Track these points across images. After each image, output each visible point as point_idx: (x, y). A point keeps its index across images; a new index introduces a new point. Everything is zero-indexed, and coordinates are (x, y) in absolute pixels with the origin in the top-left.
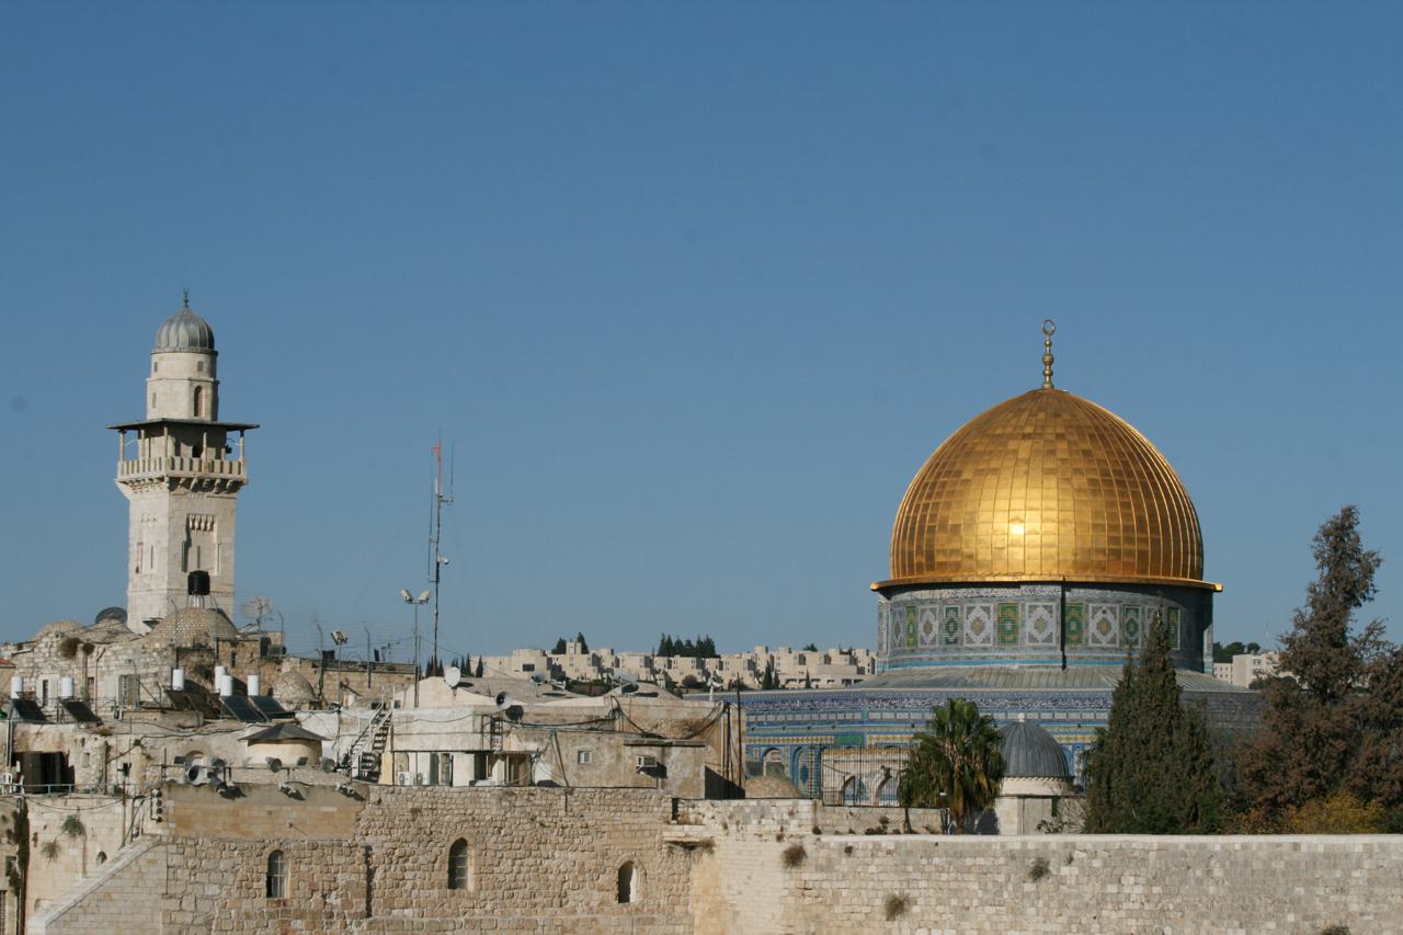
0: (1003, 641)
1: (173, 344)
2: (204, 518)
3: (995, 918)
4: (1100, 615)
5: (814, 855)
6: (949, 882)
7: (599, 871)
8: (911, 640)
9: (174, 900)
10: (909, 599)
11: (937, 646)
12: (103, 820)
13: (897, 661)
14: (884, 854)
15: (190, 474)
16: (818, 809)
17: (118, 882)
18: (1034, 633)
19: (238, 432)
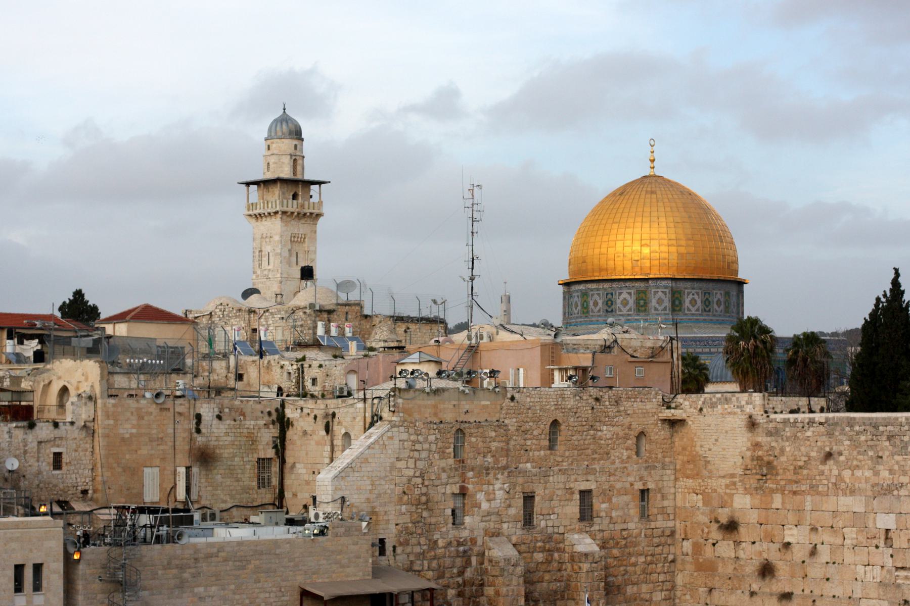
0: (639, 311)
1: (280, 134)
2: (300, 236)
3: (902, 463)
4: (691, 296)
5: (765, 426)
6: (867, 441)
7: (626, 438)
8: (585, 311)
9: (403, 462)
10: (584, 288)
11: (601, 313)
12: (348, 412)
13: (577, 322)
14: (818, 425)
15: (293, 210)
16: (766, 398)
17: (371, 451)
18: (657, 306)
19: (318, 186)
